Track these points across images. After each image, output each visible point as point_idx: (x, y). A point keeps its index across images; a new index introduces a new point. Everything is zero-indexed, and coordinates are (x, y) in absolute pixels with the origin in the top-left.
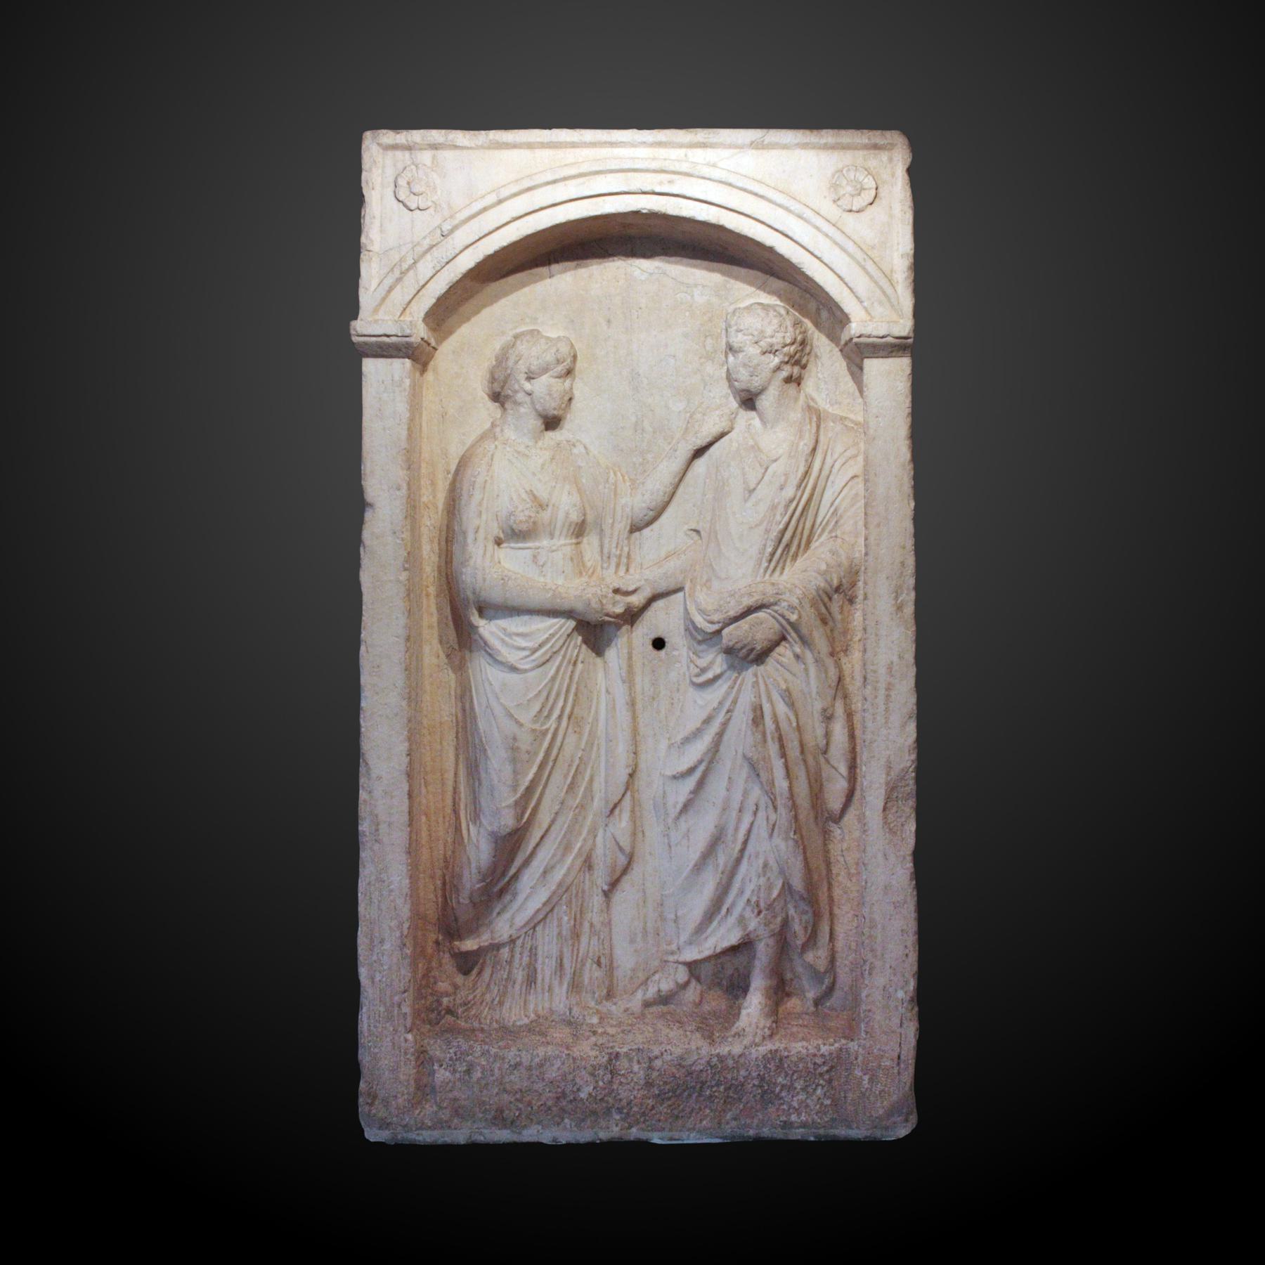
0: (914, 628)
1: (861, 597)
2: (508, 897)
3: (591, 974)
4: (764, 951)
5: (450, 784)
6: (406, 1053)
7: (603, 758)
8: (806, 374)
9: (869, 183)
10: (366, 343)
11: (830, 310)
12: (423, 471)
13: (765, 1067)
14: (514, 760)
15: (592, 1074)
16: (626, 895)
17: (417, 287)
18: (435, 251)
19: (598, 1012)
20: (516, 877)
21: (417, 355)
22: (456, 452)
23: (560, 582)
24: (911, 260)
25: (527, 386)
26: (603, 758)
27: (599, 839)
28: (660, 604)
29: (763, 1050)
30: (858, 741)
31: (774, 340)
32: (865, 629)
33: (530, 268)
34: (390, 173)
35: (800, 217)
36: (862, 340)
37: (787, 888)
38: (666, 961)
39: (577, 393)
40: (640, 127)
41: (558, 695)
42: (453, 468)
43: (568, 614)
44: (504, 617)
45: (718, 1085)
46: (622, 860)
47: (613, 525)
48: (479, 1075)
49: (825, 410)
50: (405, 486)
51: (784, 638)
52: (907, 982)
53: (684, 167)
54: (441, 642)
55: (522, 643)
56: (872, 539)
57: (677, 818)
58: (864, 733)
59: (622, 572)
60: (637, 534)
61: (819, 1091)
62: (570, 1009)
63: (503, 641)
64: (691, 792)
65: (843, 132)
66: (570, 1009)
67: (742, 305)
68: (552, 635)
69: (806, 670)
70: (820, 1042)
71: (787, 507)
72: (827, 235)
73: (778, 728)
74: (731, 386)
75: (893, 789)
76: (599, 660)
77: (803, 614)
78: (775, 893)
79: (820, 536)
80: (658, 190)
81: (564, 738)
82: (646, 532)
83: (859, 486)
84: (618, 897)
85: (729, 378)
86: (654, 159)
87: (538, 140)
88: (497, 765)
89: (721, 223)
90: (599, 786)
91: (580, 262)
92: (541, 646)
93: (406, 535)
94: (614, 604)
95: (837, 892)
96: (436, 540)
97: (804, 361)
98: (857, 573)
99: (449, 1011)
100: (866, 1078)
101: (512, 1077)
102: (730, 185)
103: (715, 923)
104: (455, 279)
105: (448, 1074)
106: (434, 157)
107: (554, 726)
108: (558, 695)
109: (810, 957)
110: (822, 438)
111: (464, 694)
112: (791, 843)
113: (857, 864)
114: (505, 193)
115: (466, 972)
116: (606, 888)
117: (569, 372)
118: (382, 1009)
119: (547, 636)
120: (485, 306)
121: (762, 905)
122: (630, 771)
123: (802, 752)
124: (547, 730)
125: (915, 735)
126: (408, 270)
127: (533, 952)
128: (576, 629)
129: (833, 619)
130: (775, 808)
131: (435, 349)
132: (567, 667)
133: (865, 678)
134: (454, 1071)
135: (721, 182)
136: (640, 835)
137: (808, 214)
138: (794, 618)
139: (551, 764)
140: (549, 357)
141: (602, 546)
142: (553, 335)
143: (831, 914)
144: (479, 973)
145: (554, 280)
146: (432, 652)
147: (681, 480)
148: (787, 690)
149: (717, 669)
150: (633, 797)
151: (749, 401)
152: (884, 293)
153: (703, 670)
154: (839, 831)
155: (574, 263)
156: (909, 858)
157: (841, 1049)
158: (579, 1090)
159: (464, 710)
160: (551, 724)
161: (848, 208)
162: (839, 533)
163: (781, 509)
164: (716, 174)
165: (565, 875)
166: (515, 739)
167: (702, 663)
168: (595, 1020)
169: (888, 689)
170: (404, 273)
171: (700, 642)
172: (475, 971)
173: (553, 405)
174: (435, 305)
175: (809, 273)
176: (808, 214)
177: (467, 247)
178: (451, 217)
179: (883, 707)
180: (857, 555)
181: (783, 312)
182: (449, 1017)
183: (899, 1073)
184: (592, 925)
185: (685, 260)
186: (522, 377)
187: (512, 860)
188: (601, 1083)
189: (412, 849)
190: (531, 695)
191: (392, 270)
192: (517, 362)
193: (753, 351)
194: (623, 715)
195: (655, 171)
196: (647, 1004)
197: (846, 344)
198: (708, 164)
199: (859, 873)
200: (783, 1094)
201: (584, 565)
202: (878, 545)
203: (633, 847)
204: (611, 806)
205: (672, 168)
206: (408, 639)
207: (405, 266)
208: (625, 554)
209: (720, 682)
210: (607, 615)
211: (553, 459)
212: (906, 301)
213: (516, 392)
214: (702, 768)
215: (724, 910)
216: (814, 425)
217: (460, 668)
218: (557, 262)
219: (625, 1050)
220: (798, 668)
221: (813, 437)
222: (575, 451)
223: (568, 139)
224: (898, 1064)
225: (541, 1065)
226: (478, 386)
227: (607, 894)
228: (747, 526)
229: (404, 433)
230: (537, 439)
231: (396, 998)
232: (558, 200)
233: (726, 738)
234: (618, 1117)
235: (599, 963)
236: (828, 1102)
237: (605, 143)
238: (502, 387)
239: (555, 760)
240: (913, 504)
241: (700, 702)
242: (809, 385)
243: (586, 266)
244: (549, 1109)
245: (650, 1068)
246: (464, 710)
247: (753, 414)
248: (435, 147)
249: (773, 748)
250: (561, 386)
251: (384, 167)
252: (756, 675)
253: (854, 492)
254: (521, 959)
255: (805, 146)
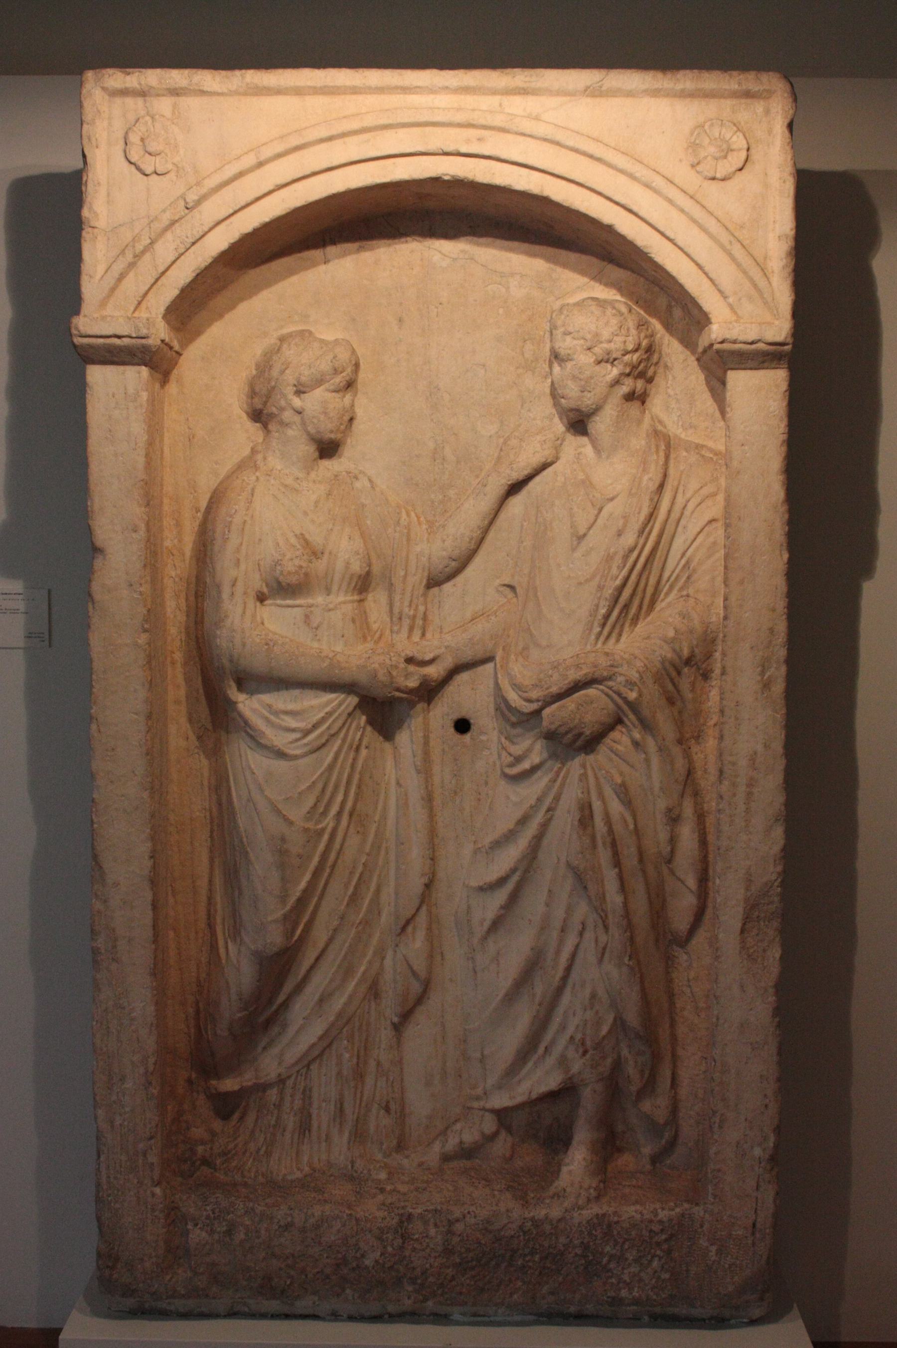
0: (784, 711)
1: (717, 671)
2: (276, 1029)
3: (378, 1121)
4: (590, 1099)
5: (204, 892)
6: (153, 1210)
7: (393, 865)
8: (652, 390)
9: (739, 141)
10: (91, 346)
11: (685, 308)
12: (166, 508)
13: (590, 1234)
14: (282, 866)
15: (380, 1239)
16: (421, 1029)
17: (155, 275)
18: (178, 229)
19: (386, 1166)
20: (285, 1005)
21: (158, 362)
22: (206, 483)
23: (339, 648)
24: (791, 243)
25: (297, 402)
26: (393, 865)
27: (388, 962)
28: (464, 676)
29: (587, 1213)
30: (711, 848)
31: (612, 346)
32: (722, 712)
33: (300, 250)
34: (119, 127)
35: (647, 186)
36: (725, 346)
37: (620, 1023)
38: (470, 1108)
39: (359, 412)
40: (442, 67)
41: (336, 787)
42: (203, 504)
43: (349, 688)
44: (269, 691)
45: (533, 1253)
46: (416, 988)
47: (405, 576)
48: (242, 1236)
49: (676, 436)
50: (143, 526)
51: (619, 721)
52: (765, 1138)
53: (498, 120)
54: (190, 720)
55: (292, 723)
56: (733, 599)
57: (485, 938)
58: (718, 838)
59: (416, 637)
60: (436, 590)
61: (655, 1263)
62: (353, 1163)
63: (268, 720)
64: (502, 907)
65: (705, 74)
66: (353, 1163)
67: (572, 300)
68: (329, 714)
69: (647, 761)
70: (658, 1205)
71: (626, 557)
72: (682, 211)
73: (611, 831)
74: (556, 404)
75: (754, 907)
76: (387, 746)
77: (645, 691)
78: (605, 1030)
79: (667, 594)
80: (463, 150)
81: (344, 839)
82: (447, 587)
83: (718, 533)
84: (411, 1031)
85: (554, 394)
86: (459, 109)
87: (309, 83)
88: (261, 868)
89: (545, 194)
90: (388, 891)
91: (364, 243)
92: (315, 727)
93: (146, 588)
94: (407, 676)
95: (681, 1030)
96: (183, 595)
97: (650, 373)
98: (714, 641)
99: (205, 1162)
100: (713, 1249)
101: (282, 1240)
102: (558, 144)
103: (530, 1064)
104: (203, 265)
105: (204, 1234)
106: (175, 106)
107: (331, 825)
108: (336, 787)
109: (646, 1106)
110: (672, 471)
111: (220, 784)
112: (625, 969)
113: (707, 996)
114: (267, 153)
115: (226, 1117)
116: (396, 1020)
117: (350, 385)
118: (124, 1158)
119: (322, 714)
120: (242, 299)
121: (588, 1043)
122: (425, 880)
123: (641, 860)
124: (323, 830)
125: (782, 842)
126: (143, 252)
127: (307, 1094)
128: (359, 706)
129: (683, 700)
130: (606, 928)
131: (179, 354)
132: (347, 753)
133: (721, 772)
134: (212, 1232)
135: (545, 140)
136: (439, 958)
137: (659, 182)
138: (633, 696)
139: (328, 870)
140: (325, 365)
141: (391, 605)
142: (329, 336)
143: (674, 1055)
144: (242, 1118)
145: (330, 266)
146: (179, 733)
147: (491, 523)
148: (623, 785)
149: (535, 758)
150: (430, 912)
151: (579, 423)
152: (755, 286)
153: (518, 760)
154: (685, 957)
155: (356, 245)
156: (771, 991)
157: (683, 1215)
158: (363, 1256)
159: (220, 805)
160: (329, 822)
161: (711, 175)
162: (691, 591)
163: (618, 560)
164: (541, 129)
165: (346, 1004)
166: (283, 839)
167: (517, 750)
168: (383, 1176)
169: (750, 785)
170: (138, 256)
171: (514, 725)
172: (236, 1115)
173: (330, 426)
174: (178, 297)
175: (659, 259)
176: (659, 182)
177: (218, 223)
178: (198, 184)
179: (742, 807)
180: (714, 619)
181: (624, 309)
182: (205, 1170)
183: (754, 1244)
184: (379, 1064)
185: (499, 242)
186: (289, 391)
187: (281, 985)
188: (390, 1249)
189: (158, 970)
190: (303, 787)
191: (123, 252)
192: (282, 372)
193: (586, 359)
194: (417, 813)
195: (460, 125)
196: (446, 1158)
197: (705, 351)
198: (529, 117)
199: (709, 1007)
200: (612, 1266)
201: (369, 628)
202: (741, 606)
203: (430, 971)
204: (403, 922)
205: (482, 122)
206: (149, 717)
207: (139, 247)
208: (420, 614)
209: (539, 773)
210: (398, 689)
211: (329, 494)
212: (783, 294)
213: (282, 409)
214: (515, 878)
215: (541, 1050)
216: (662, 454)
217: (215, 753)
218: (334, 242)
219: (419, 1211)
220: (637, 758)
221: (661, 470)
222: (358, 485)
223: (348, 83)
224: (753, 1234)
225: (317, 1227)
226: (234, 402)
227: (398, 1028)
228: (575, 582)
229: (141, 461)
230: (308, 469)
231: (141, 1146)
232: (336, 163)
233: (545, 841)
234: (410, 1288)
235: (387, 1109)
236: (667, 1276)
237: (396, 88)
238: (265, 403)
239: (333, 867)
240: (786, 556)
241: (514, 798)
242: (657, 404)
243: (372, 249)
244: (328, 1277)
245: (450, 1232)
246: (220, 805)
247: (584, 440)
248: (175, 92)
249: (604, 855)
250: (338, 403)
251: (110, 118)
252: (584, 766)
253: (711, 539)
254: (292, 1102)
255: (655, 93)
